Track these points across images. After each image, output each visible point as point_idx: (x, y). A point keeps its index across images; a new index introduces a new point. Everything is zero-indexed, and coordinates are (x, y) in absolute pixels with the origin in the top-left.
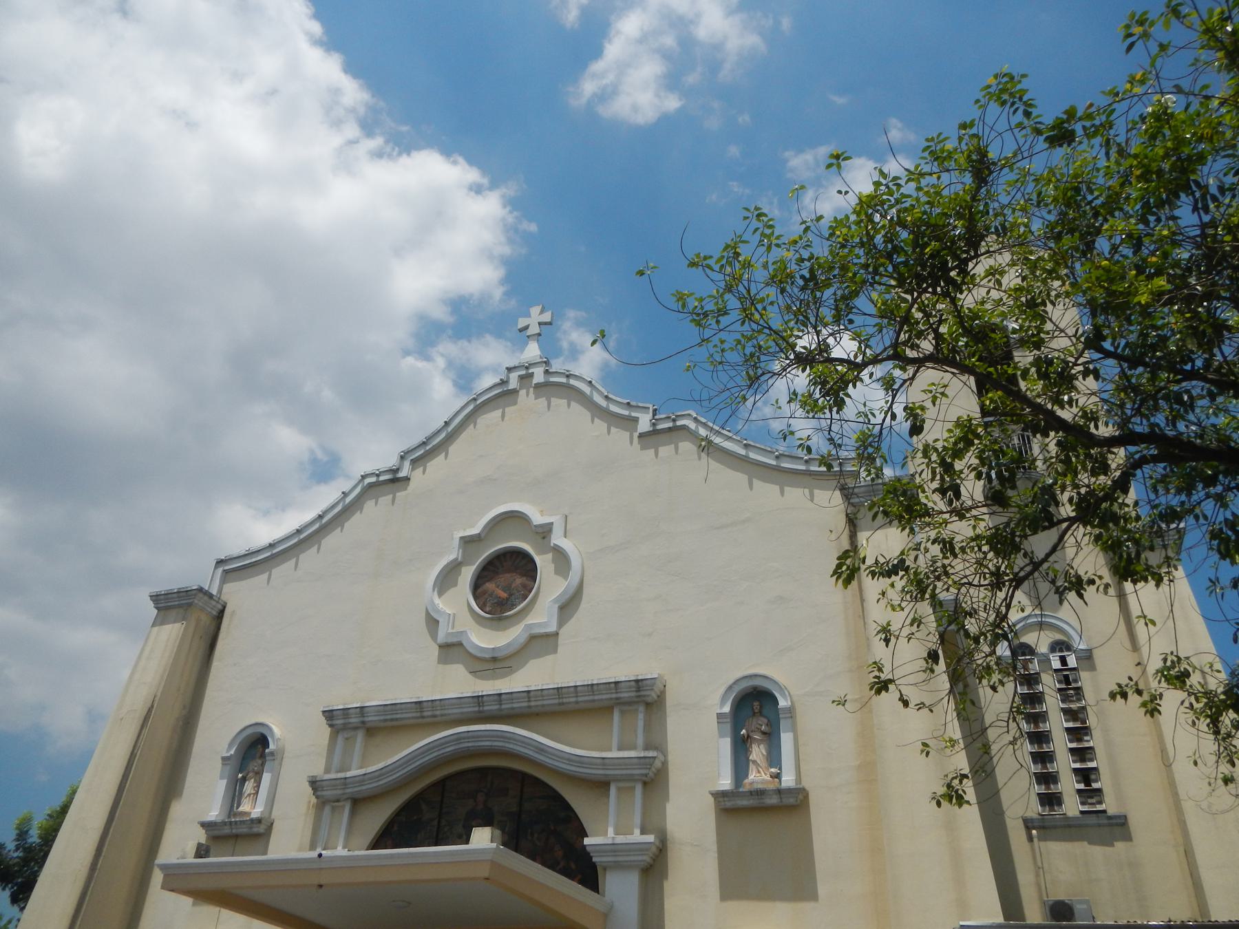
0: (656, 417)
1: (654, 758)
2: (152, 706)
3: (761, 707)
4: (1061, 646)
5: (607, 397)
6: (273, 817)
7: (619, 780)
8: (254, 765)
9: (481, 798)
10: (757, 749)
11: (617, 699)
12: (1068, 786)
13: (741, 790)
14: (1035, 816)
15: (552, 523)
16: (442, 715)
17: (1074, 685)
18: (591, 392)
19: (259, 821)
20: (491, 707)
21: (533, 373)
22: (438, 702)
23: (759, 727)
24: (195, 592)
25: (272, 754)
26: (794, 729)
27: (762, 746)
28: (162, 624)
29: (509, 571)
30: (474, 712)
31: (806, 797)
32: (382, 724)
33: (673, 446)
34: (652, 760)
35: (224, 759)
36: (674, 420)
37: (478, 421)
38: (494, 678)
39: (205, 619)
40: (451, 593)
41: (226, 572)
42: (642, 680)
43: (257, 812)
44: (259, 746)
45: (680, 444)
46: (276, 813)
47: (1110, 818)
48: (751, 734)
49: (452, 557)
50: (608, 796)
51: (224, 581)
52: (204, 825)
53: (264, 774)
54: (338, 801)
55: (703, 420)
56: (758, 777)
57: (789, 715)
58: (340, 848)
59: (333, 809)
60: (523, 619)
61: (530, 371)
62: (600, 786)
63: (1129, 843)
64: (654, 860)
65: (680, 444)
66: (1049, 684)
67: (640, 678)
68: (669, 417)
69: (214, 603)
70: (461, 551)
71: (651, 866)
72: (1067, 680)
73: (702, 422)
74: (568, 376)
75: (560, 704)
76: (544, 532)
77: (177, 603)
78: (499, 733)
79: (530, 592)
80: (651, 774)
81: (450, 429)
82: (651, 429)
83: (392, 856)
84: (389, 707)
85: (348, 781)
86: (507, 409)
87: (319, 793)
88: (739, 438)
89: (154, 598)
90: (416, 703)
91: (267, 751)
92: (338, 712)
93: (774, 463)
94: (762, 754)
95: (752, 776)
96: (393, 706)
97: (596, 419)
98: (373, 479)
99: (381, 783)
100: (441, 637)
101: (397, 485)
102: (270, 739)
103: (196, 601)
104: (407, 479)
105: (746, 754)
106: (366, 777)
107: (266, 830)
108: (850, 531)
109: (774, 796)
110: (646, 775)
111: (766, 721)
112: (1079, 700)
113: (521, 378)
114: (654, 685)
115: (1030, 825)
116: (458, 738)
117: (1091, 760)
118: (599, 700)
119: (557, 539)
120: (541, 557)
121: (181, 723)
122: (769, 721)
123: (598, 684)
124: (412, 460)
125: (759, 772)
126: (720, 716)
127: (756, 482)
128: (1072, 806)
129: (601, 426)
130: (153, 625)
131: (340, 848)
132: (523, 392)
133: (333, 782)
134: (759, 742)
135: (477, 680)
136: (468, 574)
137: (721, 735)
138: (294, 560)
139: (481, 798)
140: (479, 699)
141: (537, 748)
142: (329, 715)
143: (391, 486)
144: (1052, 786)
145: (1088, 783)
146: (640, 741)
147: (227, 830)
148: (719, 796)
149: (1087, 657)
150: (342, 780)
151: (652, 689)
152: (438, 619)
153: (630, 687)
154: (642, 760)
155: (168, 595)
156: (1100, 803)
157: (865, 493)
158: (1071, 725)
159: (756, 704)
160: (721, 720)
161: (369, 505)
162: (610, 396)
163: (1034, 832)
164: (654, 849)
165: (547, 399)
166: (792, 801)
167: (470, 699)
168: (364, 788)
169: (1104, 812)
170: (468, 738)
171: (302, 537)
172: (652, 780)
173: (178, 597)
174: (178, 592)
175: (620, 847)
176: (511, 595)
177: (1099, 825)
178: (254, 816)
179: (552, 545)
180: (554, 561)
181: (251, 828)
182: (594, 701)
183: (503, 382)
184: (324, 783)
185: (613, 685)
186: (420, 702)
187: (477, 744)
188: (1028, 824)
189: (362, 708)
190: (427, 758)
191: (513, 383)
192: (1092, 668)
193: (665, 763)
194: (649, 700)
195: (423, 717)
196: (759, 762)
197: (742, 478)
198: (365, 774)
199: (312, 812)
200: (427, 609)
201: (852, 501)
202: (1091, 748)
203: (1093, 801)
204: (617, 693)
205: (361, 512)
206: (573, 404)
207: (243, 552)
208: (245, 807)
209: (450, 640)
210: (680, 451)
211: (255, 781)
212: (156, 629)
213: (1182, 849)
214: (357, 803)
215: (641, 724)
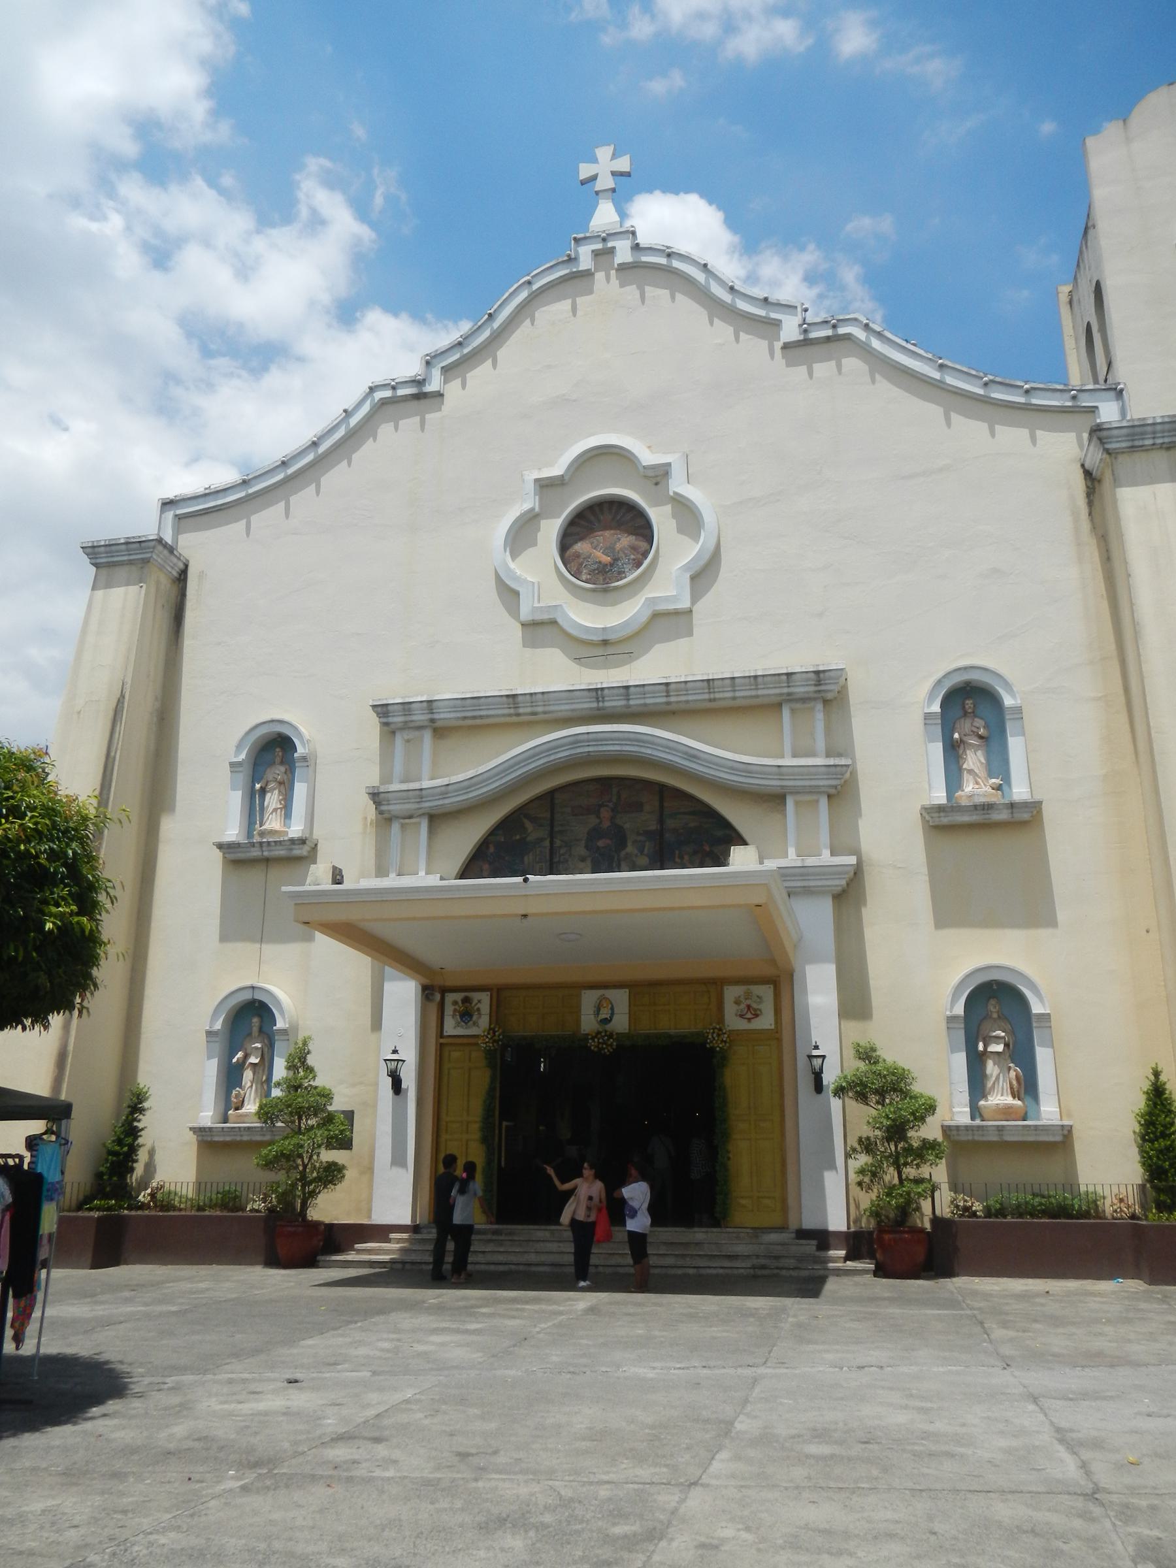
1: (847, 766)
2: (122, 696)
6: (315, 837)
7: (798, 793)
8: (279, 771)
9: (605, 813)
10: (973, 756)
11: (789, 694)
15: (669, 464)
16: (545, 713)
18: (707, 279)
19: (303, 841)
20: (611, 704)
21: (614, 248)
22: (540, 696)
23: (975, 730)
24: (153, 543)
25: (304, 759)
27: (979, 753)
28: (108, 585)
29: (606, 528)
30: (591, 709)
31: (1040, 812)
32: (461, 723)
34: (845, 768)
35: (232, 765)
36: (834, 327)
37: (537, 314)
38: (606, 666)
39: (165, 582)
40: (529, 554)
41: (179, 518)
42: (824, 671)
43: (296, 829)
45: (845, 361)
46: (317, 834)
48: (965, 739)
49: (527, 506)
50: (783, 812)
51: (177, 532)
52: (220, 846)
53: (297, 785)
54: (410, 817)
55: (878, 329)
58: (422, 873)
59: (403, 826)
60: (642, 588)
61: (610, 244)
62: (774, 800)
64: (848, 884)
65: (845, 361)
67: (821, 668)
69: (175, 560)
70: (537, 497)
73: (874, 331)
74: (669, 255)
75: (710, 700)
76: (657, 476)
77: (125, 558)
78: (632, 736)
79: (645, 554)
81: (496, 324)
82: (801, 337)
83: (629, 879)
84: (468, 702)
85: (424, 792)
86: (579, 300)
87: (384, 808)
88: (930, 356)
89: (89, 550)
90: (508, 696)
91: (296, 755)
92: (396, 706)
93: (981, 391)
94: (980, 761)
95: (969, 787)
96: (475, 701)
97: (716, 320)
98: (388, 393)
99: (471, 795)
100: (525, 613)
101: (423, 403)
102: (295, 740)
103: (155, 557)
104: (439, 395)
105: (958, 762)
106: (450, 787)
107: (309, 852)
108: (1087, 487)
109: (1005, 811)
110: (835, 787)
113: (596, 254)
114: (838, 679)
116: (576, 741)
118: (763, 696)
120: (654, 509)
121: (155, 719)
123: (763, 676)
124: (442, 368)
125: (977, 783)
126: (928, 716)
127: (954, 416)
129: (723, 330)
130: (94, 588)
131: (422, 873)
132: (600, 276)
133: (404, 794)
134: (976, 748)
135: (583, 668)
136: (551, 529)
137: (931, 741)
138: (282, 504)
139: (605, 813)
140: (598, 693)
141: (686, 753)
142: (382, 710)
143: (414, 404)
146: (821, 745)
147: (255, 853)
150: (417, 792)
152: (517, 588)
153: (808, 680)
155: (110, 546)
157: (1128, 435)
161: (385, 430)
165: (638, 288)
166: (1026, 816)
167: (586, 693)
168: (446, 801)
170: (588, 741)
171: (290, 471)
173: (127, 550)
174: (127, 543)
175: (811, 870)
176: (616, 560)
178: (291, 835)
179: (671, 494)
180: (674, 516)
181: (291, 849)
182: (757, 696)
184: (389, 795)
185: (785, 677)
186: (514, 696)
187: (601, 748)
189: (430, 702)
190: (533, 766)
191: (585, 261)
193: (854, 774)
194: (829, 696)
195: (518, 715)
196: (977, 771)
197: (934, 411)
198: (448, 785)
199: (371, 830)
200: (498, 578)
201: (1108, 446)
204: (789, 687)
205: (375, 440)
206: (679, 296)
207: (201, 491)
208: (273, 823)
209: (539, 617)
210: (844, 370)
211: (280, 791)
212: (100, 593)
214: (436, 819)
215: (820, 726)
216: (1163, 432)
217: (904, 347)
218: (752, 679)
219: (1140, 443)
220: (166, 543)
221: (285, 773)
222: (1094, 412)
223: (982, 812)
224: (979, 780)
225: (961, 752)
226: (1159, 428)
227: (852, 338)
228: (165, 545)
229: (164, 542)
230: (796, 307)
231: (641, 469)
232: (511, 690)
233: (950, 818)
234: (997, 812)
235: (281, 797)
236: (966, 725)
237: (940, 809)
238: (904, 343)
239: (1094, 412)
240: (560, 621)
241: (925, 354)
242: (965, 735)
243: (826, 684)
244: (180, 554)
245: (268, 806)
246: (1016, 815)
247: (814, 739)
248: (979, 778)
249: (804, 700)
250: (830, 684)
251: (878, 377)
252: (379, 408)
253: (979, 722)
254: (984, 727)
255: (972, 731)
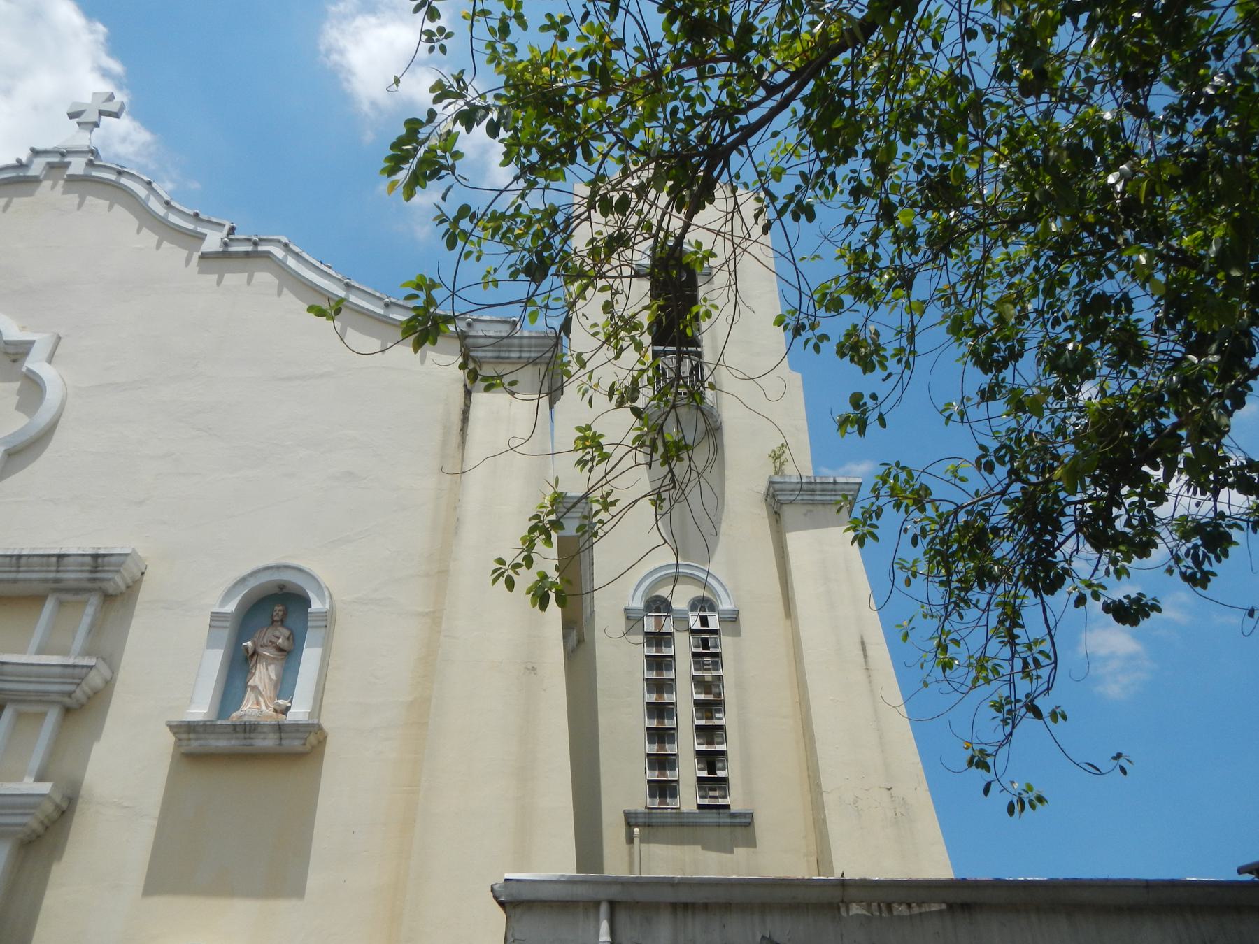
0: (232, 237)
1: (91, 667)
3: (285, 614)
4: (703, 605)
5: (167, 203)
11: (57, 581)
12: (688, 772)
13: (219, 722)
14: (641, 809)
15: (32, 343)
17: (712, 650)
23: (274, 639)
26: (326, 645)
27: (272, 668)
31: (322, 741)
33: (246, 275)
34: (85, 670)
36: (256, 244)
42: (104, 556)
47: (734, 815)
48: (260, 650)
55: (297, 249)
56: (254, 708)
57: (324, 623)
61: (67, 160)
63: (752, 849)
66: (683, 647)
67: (101, 552)
68: (249, 240)
71: (39, 837)
72: (705, 644)
74: (120, 173)
76: (17, 354)
80: (79, 694)
82: (221, 250)
88: (340, 277)
93: (381, 311)
105: (246, 677)
109: (271, 735)
110: (69, 694)
111: (287, 633)
112: (717, 669)
113: (51, 166)
114: (121, 564)
115: (633, 821)
117: (722, 743)
118: (25, 580)
119: (35, 363)
122: (292, 633)
123: (29, 556)
125: (258, 703)
126: (215, 616)
128: (688, 799)
129: (149, 238)
132: (47, 184)
134: (269, 661)
137: (211, 644)
144: (668, 772)
145: (712, 769)
146: (79, 642)
148: (185, 730)
149: (733, 619)
151: (118, 571)
153: (82, 565)
154: (69, 671)
156: (725, 797)
158: (702, 697)
159: (278, 609)
160: (214, 624)
162: (173, 203)
163: (636, 830)
164: (49, 808)
166: (295, 744)
169: (727, 807)
172: (82, 706)
177: (719, 825)
179: (24, 369)
180: (19, 392)
182: (15, 581)
183: (20, 165)
185: (54, 559)
188: (630, 820)
192: (737, 633)
193: (109, 684)
194: (111, 591)
196: (261, 689)
202: (721, 728)
203: (716, 793)
204: (58, 571)
206: (117, 207)
210: (253, 282)
213: (814, 859)
215: (86, 621)
216: (530, 346)
217: (318, 268)
218: (14, 559)
219: (506, 355)
223: (242, 735)
224: (261, 699)
226: (525, 341)
230: (224, 225)
233: (202, 742)
234: (262, 736)
236: (269, 634)
238: (318, 264)
241: (335, 275)
243: (104, 571)
246: (284, 742)
248: (262, 696)
249: (77, 591)
250: (108, 571)
251: (285, 289)
254: (288, 638)
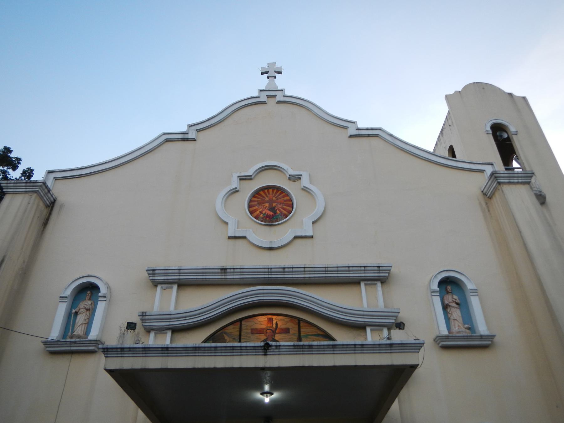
8: (87, 303)
15: (301, 175)
24: (41, 184)
41: (56, 180)
43: (93, 335)
44: (89, 292)
48: (450, 304)
56: (458, 327)
57: (476, 294)
69: (50, 196)
90: (221, 269)
91: (100, 294)
104: (194, 140)
140: (270, 270)
159: (449, 288)
160: (433, 294)
220: (48, 186)
221: (91, 304)
222: (483, 172)
225: (449, 310)
226: (520, 175)
227: (379, 136)
228: (47, 187)
229: (46, 185)
231: (288, 177)
232: (223, 266)
235: (86, 318)
237: (446, 338)
239: (483, 172)
240: (248, 237)
242: (450, 303)
244: (53, 194)
245: (78, 323)
247: (378, 301)
252: (164, 143)
253: (455, 297)
255: (453, 301)
